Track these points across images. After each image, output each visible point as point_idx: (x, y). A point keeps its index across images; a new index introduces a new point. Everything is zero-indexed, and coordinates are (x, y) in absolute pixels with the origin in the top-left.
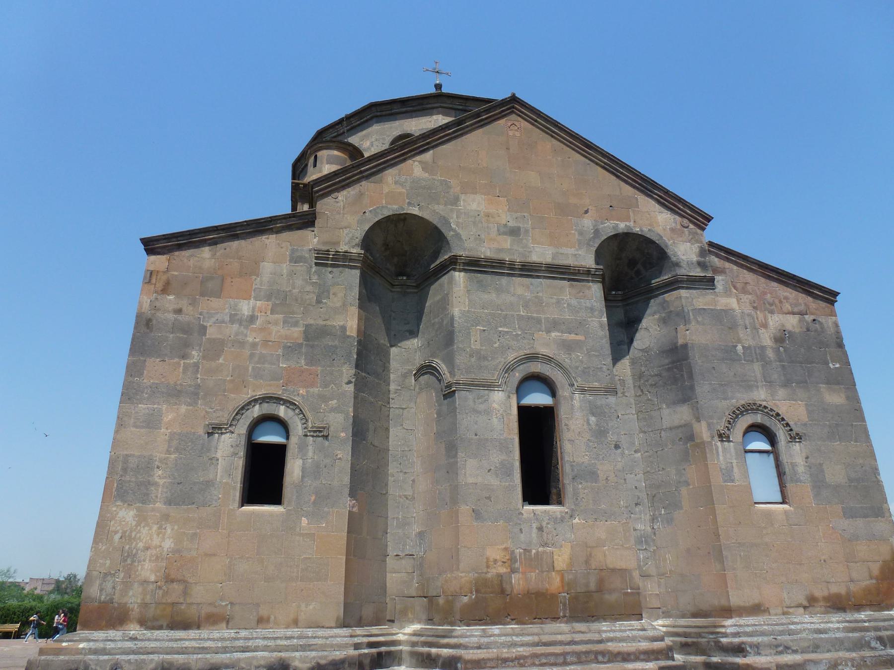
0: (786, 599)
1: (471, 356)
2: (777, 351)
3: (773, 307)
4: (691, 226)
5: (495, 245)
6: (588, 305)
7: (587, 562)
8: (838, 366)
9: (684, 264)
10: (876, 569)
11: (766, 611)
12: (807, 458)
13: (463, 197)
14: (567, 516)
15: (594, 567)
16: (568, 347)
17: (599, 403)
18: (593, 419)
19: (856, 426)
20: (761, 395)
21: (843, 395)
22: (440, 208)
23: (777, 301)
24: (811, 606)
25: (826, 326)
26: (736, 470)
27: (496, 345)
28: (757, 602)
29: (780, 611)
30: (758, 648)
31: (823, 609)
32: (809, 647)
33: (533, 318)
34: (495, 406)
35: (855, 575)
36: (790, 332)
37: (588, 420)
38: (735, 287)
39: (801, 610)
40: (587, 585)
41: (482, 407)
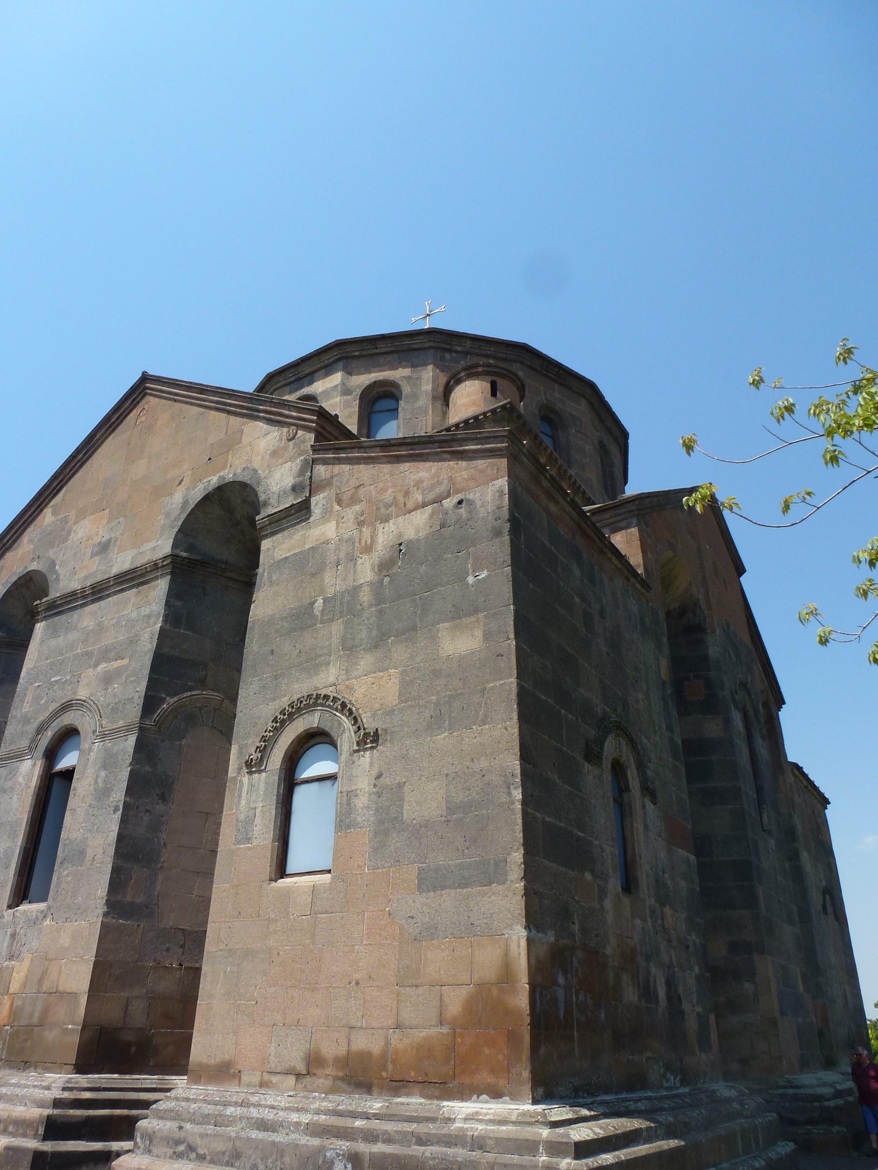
0: (272, 1058)
1: (19, 721)
2: (377, 587)
3: (393, 508)
4: (300, 433)
5: (85, 573)
6: (147, 612)
7: (40, 981)
8: (484, 575)
9: (273, 501)
10: (455, 1002)
11: (236, 1076)
12: (378, 777)
13: (74, 527)
14: (41, 916)
15: (44, 989)
16: (107, 679)
17: (116, 748)
18: (103, 774)
19: (493, 688)
20: (327, 679)
21: (479, 633)
22: (51, 554)
23: (400, 498)
24: (308, 1074)
25: (479, 503)
26: (258, 820)
27: (42, 702)
28: (227, 1057)
29: (256, 1079)
30: (151, 1141)
31: (329, 1082)
32: (224, 1153)
33: (87, 653)
34: (20, 779)
35: (408, 1015)
36: (410, 542)
37: (97, 777)
38: (339, 504)
39: (291, 1080)
40: (31, 1016)
41: (10, 784)
